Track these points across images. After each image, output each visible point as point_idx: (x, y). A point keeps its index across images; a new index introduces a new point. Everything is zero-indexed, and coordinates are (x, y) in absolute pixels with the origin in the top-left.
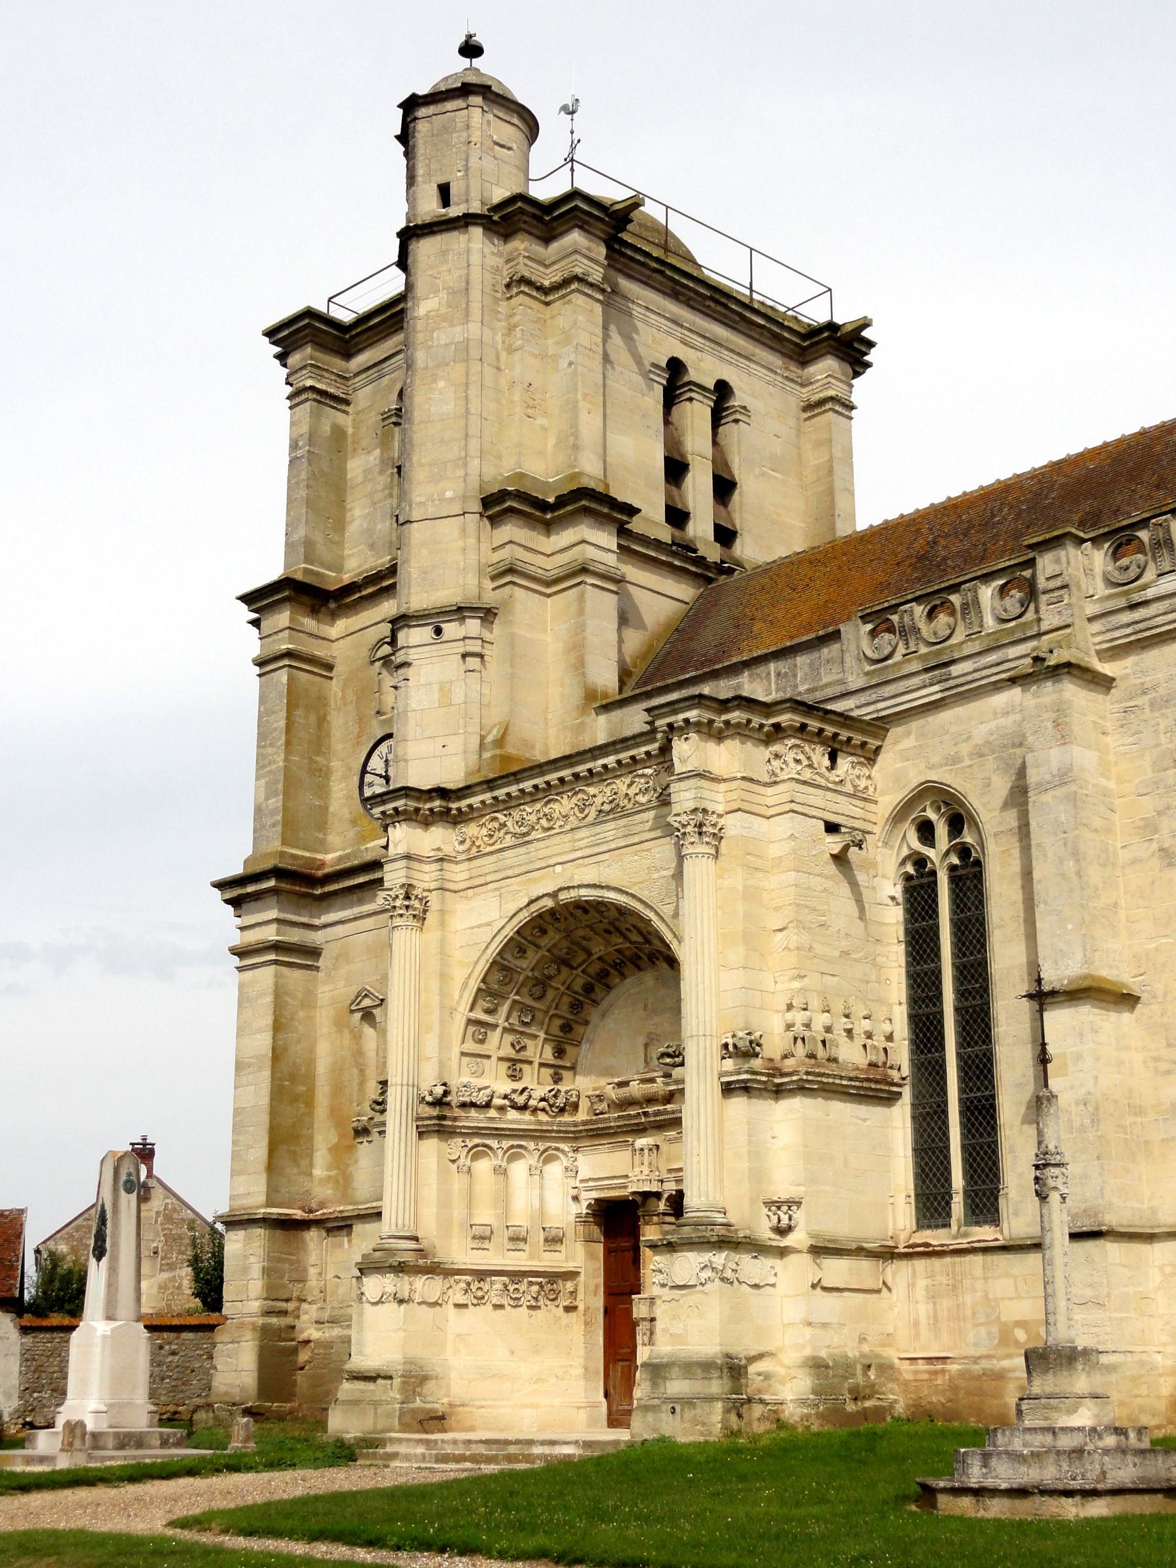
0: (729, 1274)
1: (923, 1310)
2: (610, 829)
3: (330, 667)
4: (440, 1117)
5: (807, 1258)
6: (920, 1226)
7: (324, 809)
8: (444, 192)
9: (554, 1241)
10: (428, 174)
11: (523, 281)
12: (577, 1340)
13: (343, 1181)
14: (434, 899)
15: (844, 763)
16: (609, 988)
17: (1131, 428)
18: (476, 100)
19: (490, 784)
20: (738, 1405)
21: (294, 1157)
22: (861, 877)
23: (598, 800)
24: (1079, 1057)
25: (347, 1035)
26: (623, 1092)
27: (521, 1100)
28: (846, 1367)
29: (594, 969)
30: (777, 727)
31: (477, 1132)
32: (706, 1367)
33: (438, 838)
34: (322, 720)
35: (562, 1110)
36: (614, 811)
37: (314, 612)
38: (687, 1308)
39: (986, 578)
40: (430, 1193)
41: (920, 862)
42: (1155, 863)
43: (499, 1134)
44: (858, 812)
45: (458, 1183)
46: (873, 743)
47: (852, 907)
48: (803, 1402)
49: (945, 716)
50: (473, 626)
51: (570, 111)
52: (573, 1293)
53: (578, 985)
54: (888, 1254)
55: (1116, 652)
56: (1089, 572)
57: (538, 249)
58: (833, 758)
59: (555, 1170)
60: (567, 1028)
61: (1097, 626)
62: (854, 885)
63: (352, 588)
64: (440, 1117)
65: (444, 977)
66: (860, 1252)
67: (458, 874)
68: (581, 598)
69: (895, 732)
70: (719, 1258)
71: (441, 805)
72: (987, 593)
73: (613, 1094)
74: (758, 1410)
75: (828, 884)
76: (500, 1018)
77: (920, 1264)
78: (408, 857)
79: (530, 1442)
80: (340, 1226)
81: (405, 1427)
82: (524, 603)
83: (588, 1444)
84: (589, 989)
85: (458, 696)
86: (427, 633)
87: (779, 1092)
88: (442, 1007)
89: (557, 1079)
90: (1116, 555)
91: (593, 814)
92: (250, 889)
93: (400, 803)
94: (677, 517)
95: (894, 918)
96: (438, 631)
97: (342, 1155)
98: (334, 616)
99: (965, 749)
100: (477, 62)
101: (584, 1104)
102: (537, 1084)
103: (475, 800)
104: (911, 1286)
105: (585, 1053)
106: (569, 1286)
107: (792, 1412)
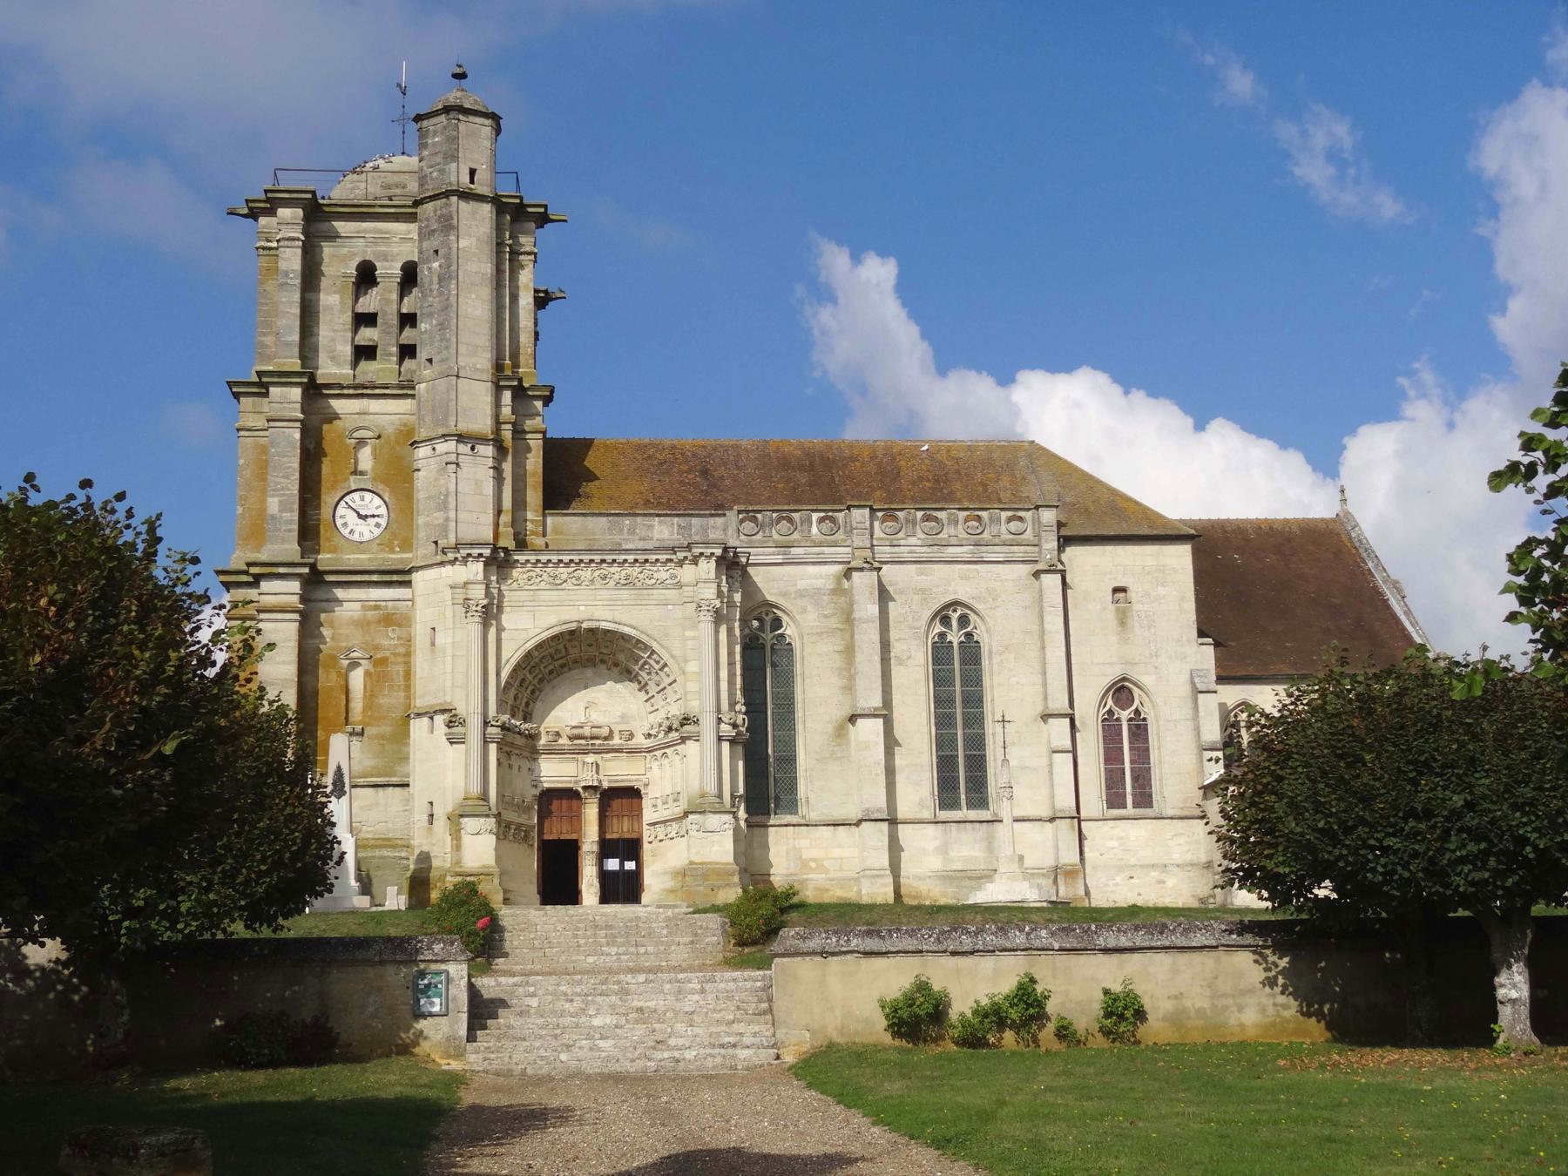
2: (625, 594)
8: (472, 172)
23: (616, 576)
84: (551, 672)
92: (282, 570)
96: (473, 448)
99: (792, 589)
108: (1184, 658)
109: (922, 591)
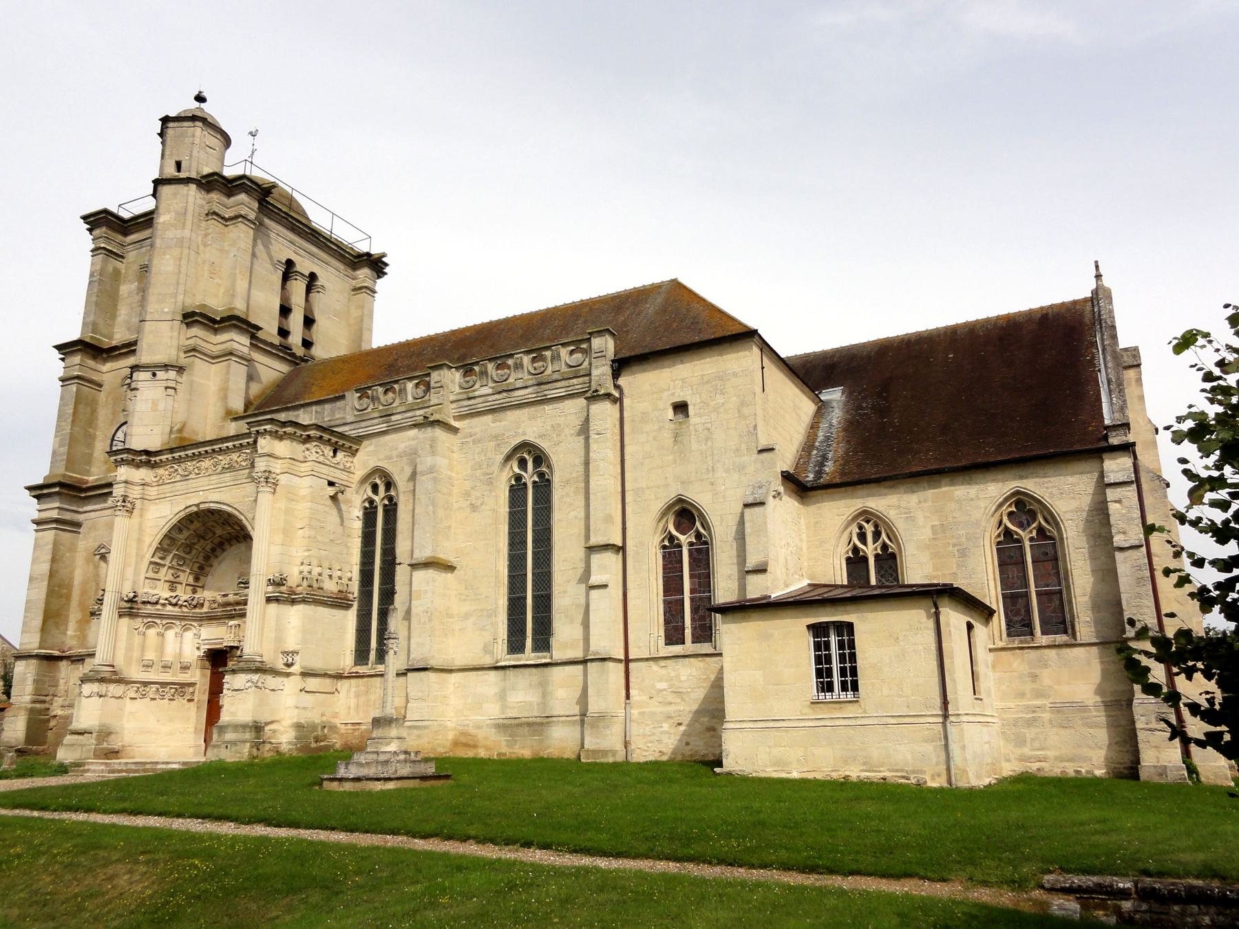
0: (260, 684)
1: (353, 702)
2: (227, 477)
3: (101, 386)
4: (131, 608)
5: (299, 678)
6: (356, 664)
7: (91, 455)
8: (179, 165)
9: (185, 668)
10: (171, 155)
11: (215, 213)
12: (194, 714)
13: (82, 637)
14: (138, 503)
15: (340, 455)
16: (224, 550)
17: (486, 320)
18: (199, 124)
19: (171, 450)
20: (257, 746)
21: (57, 625)
22: (343, 507)
24: (426, 592)
25: (91, 567)
26: (225, 599)
27: (174, 601)
28: (313, 727)
29: (217, 541)
30: (309, 436)
31: (150, 616)
32: (244, 727)
33: (143, 474)
34: (94, 411)
35: (195, 607)
36: (230, 468)
37: (94, 358)
38: (240, 702)
39: (410, 379)
40: (122, 645)
41: (371, 502)
42: (468, 510)
43: (161, 617)
44: (345, 477)
45: (137, 639)
46: (355, 447)
47: (338, 520)
48: (290, 743)
49: (388, 438)
50: (172, 374)
51: (253, 135)
52: (193, 693)
53: (208, 548)
54: (339, 676)
55: (461, 417)
56: (453, 381)
57: (224, 199)
58: (335, 452)
59: (189, 635)
60: (201, 568)
61: (454, 405)
62: (340, 510)
63: (115, 348)
64: (131, 608)
65: (140, 541)
66: (325, 675)
67: (152, 492)
68: (229, 366)
69: (365, 443)
70: (255, 677)
71: (147, 459)
72: (410, 385)
73: (220, 599)
74: (268, 747)
75: (327, 509)
76: (167, 562)
77: (353, 681)
78: (126, 482)
79: (157, 763)
80: (78, 659)
81: (96, 756)
82: (200, 366)
83: (184, 763)
84: (213, 550)
85: (161, 406)
86: (148, 375)
87: (293, 602)
88: (137, 555)
89: (194, 592)
90: (465, 375)
91: (220, 468)
93: (124, 456)
94: (283, 333)
95: (357, 526)
96: (154, 375)
97: (83, 625)
98: (105, 361)
99: (395, 453)
101: (207, 604)
102: (183, 594)
103: (163, 457)
104: (348, 691)
105: (209, 580)
106: (191, 689)
107: (285, 748)
108: (741, 468)
109: (496, 437)
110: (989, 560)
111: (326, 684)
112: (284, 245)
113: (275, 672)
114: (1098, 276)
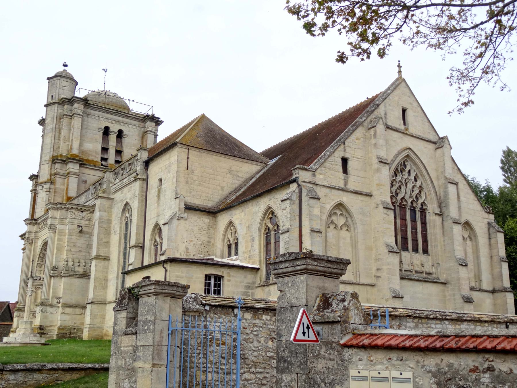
18: (59, 78)
51: (105, 70)
100: (66, 68)
110: (262, 243)
111: (78, 311)
112: (98, 121)
113: (52, 306)
114: (400, 72)
